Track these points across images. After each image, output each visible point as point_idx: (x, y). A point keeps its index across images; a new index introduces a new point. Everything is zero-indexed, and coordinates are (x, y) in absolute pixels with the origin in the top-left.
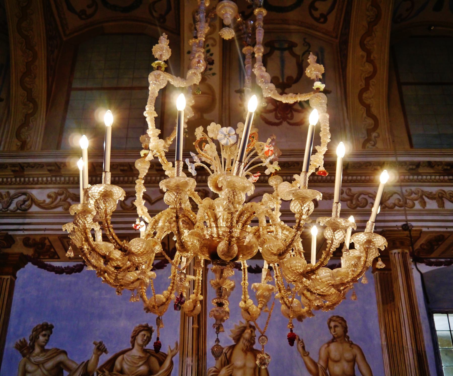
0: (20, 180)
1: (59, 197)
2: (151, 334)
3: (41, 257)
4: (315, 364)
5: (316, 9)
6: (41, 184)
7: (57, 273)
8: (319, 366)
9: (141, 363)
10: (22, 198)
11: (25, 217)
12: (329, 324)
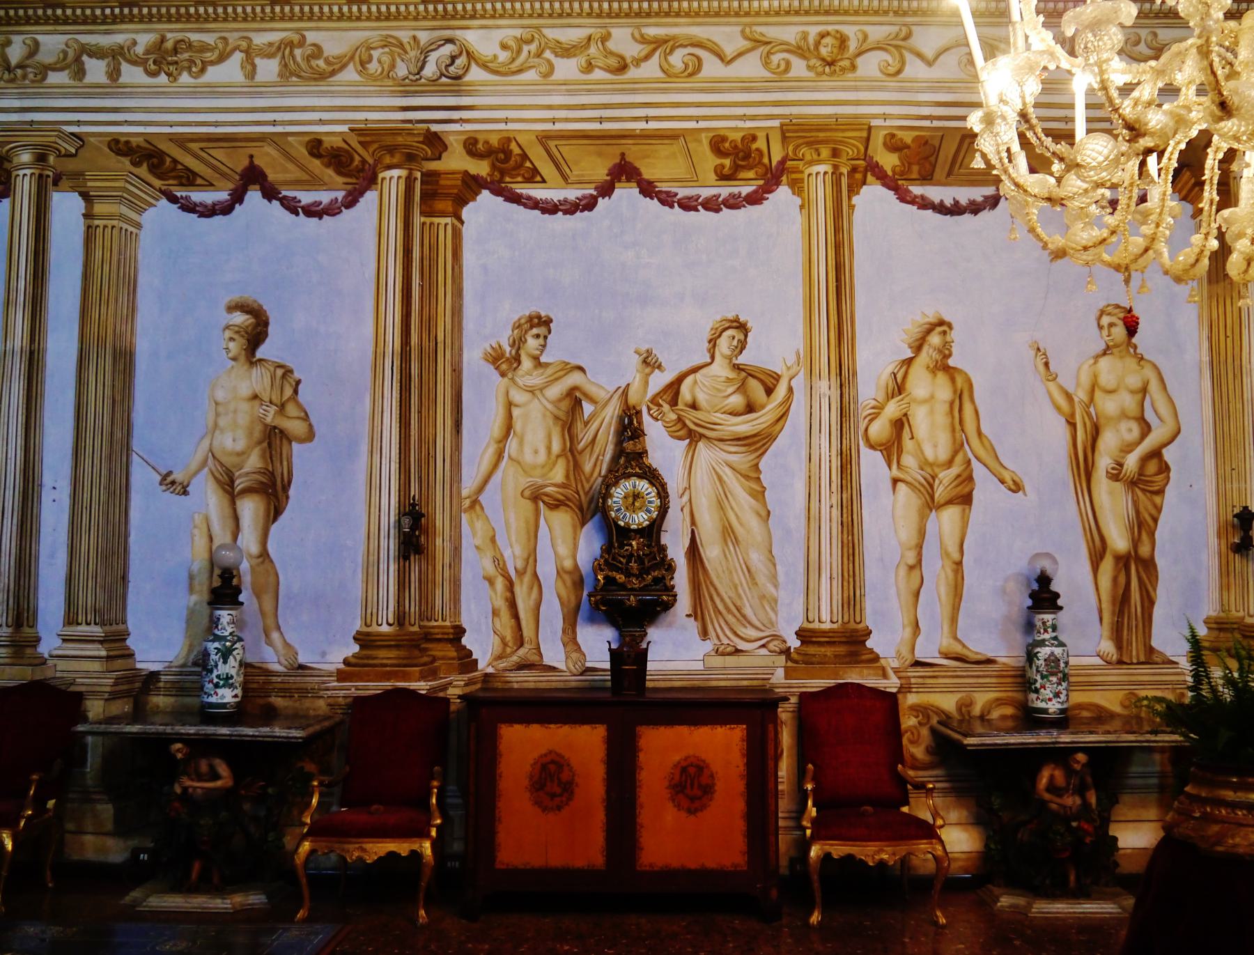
0: (436, 10)
1: (526, 48)
2: (746, 336)
3: (508, 179)
4: (1069, 397)
6: (483, 17)
7: (545, 211)
8: (1076, 399)
9: (730, 390)
10: (448, 49)
11: (458, 93)
12: (1099, 318)
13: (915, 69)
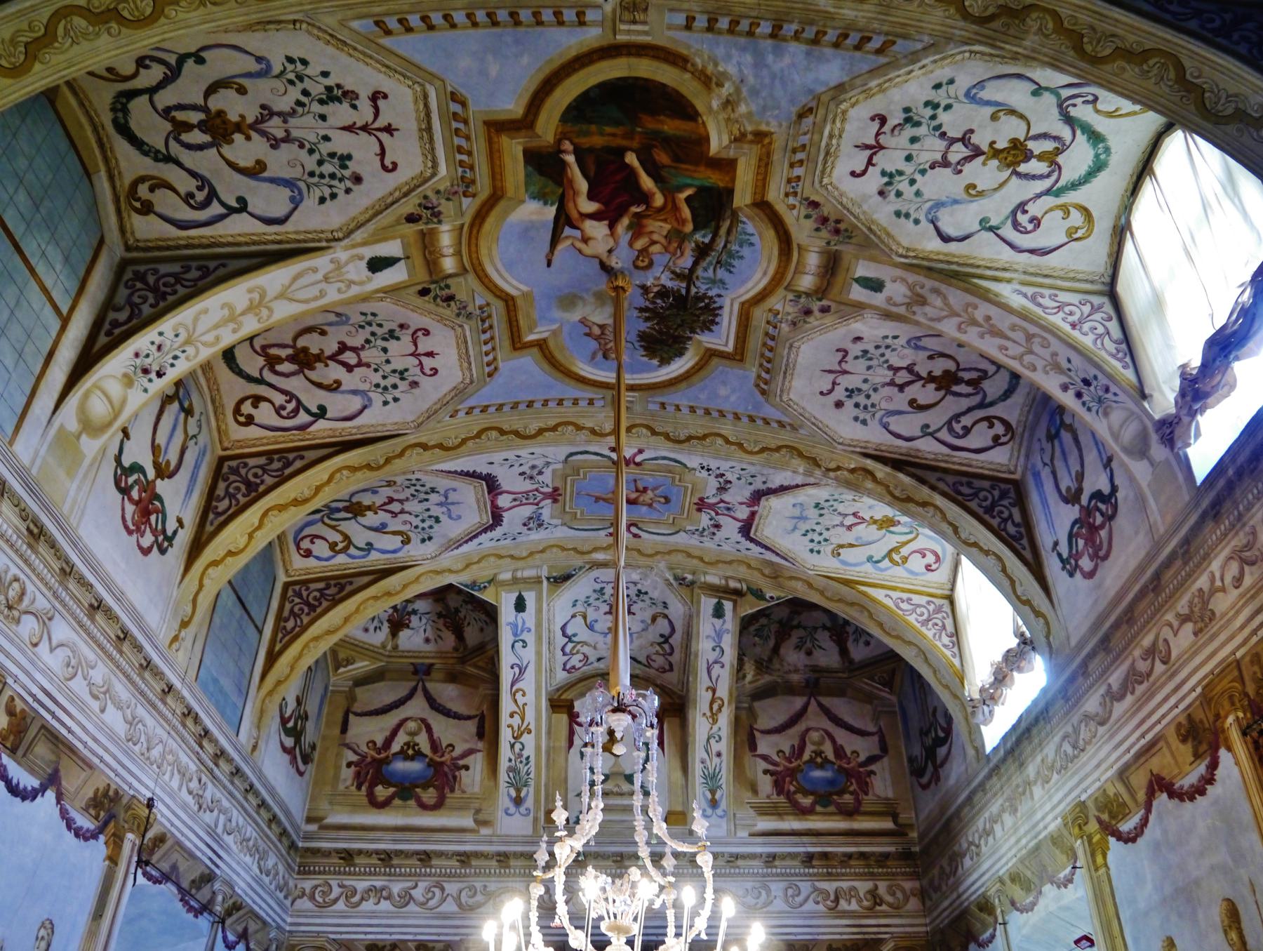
5: (255, 406)
13: (43, 648)
